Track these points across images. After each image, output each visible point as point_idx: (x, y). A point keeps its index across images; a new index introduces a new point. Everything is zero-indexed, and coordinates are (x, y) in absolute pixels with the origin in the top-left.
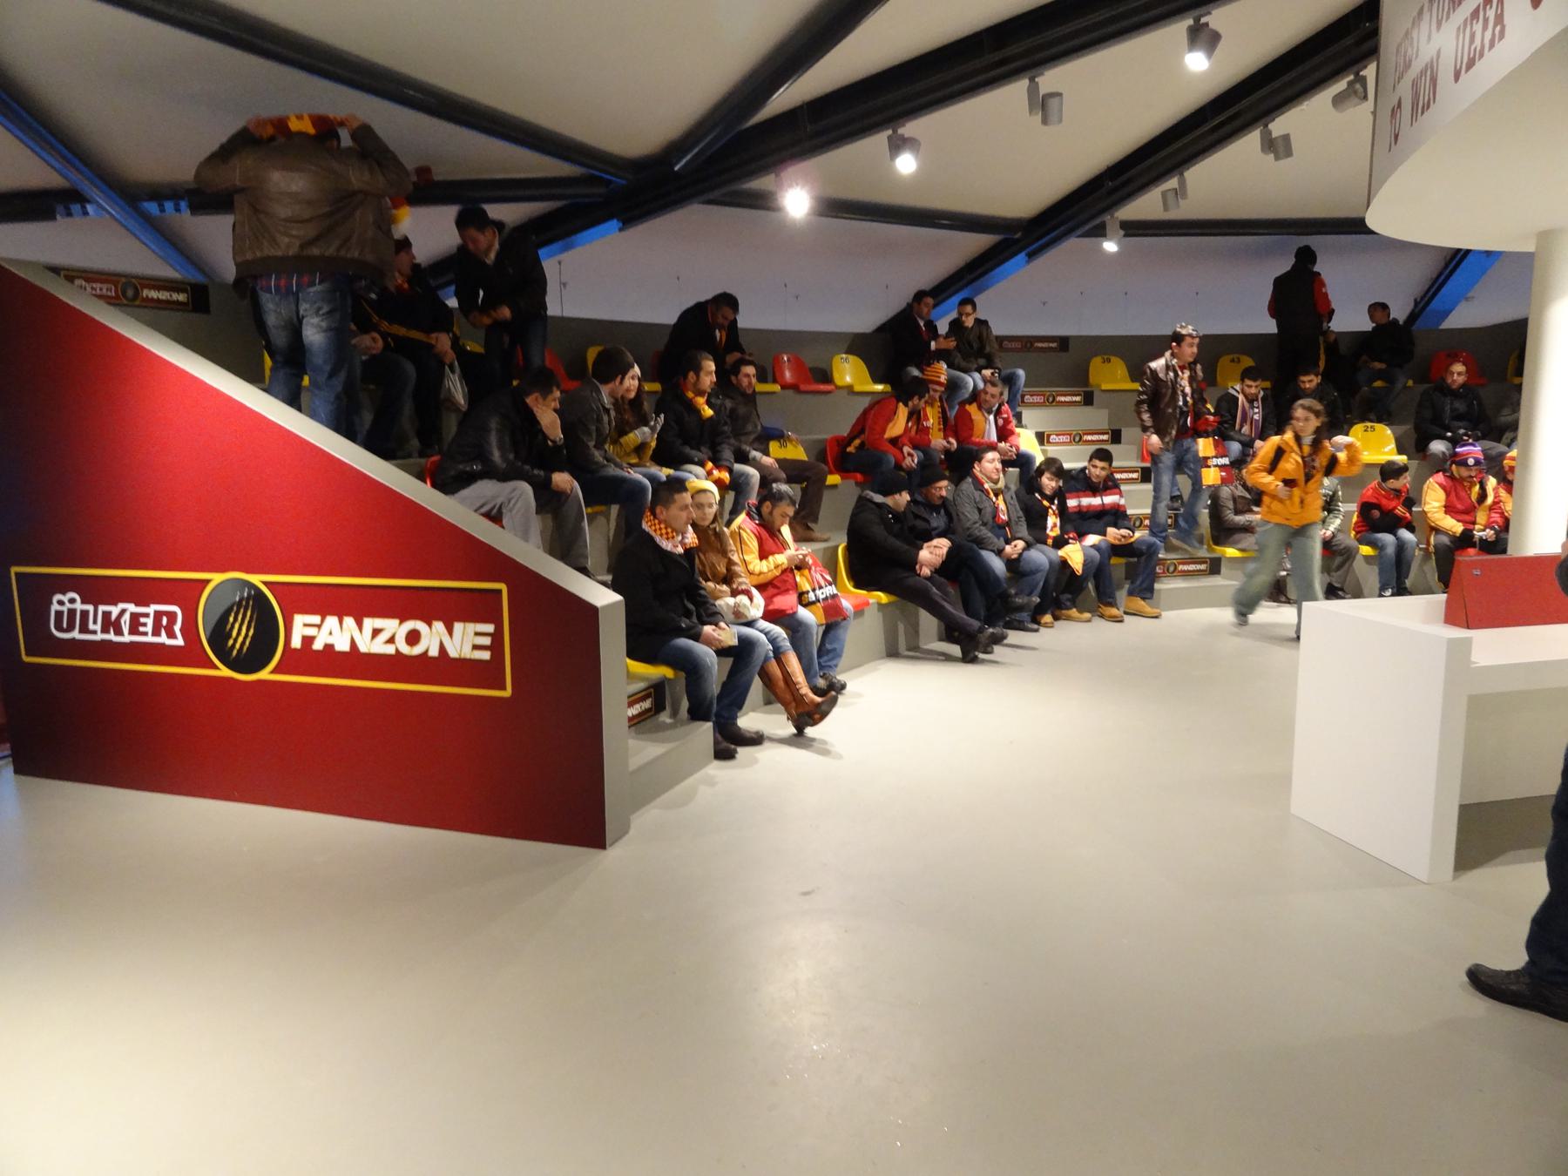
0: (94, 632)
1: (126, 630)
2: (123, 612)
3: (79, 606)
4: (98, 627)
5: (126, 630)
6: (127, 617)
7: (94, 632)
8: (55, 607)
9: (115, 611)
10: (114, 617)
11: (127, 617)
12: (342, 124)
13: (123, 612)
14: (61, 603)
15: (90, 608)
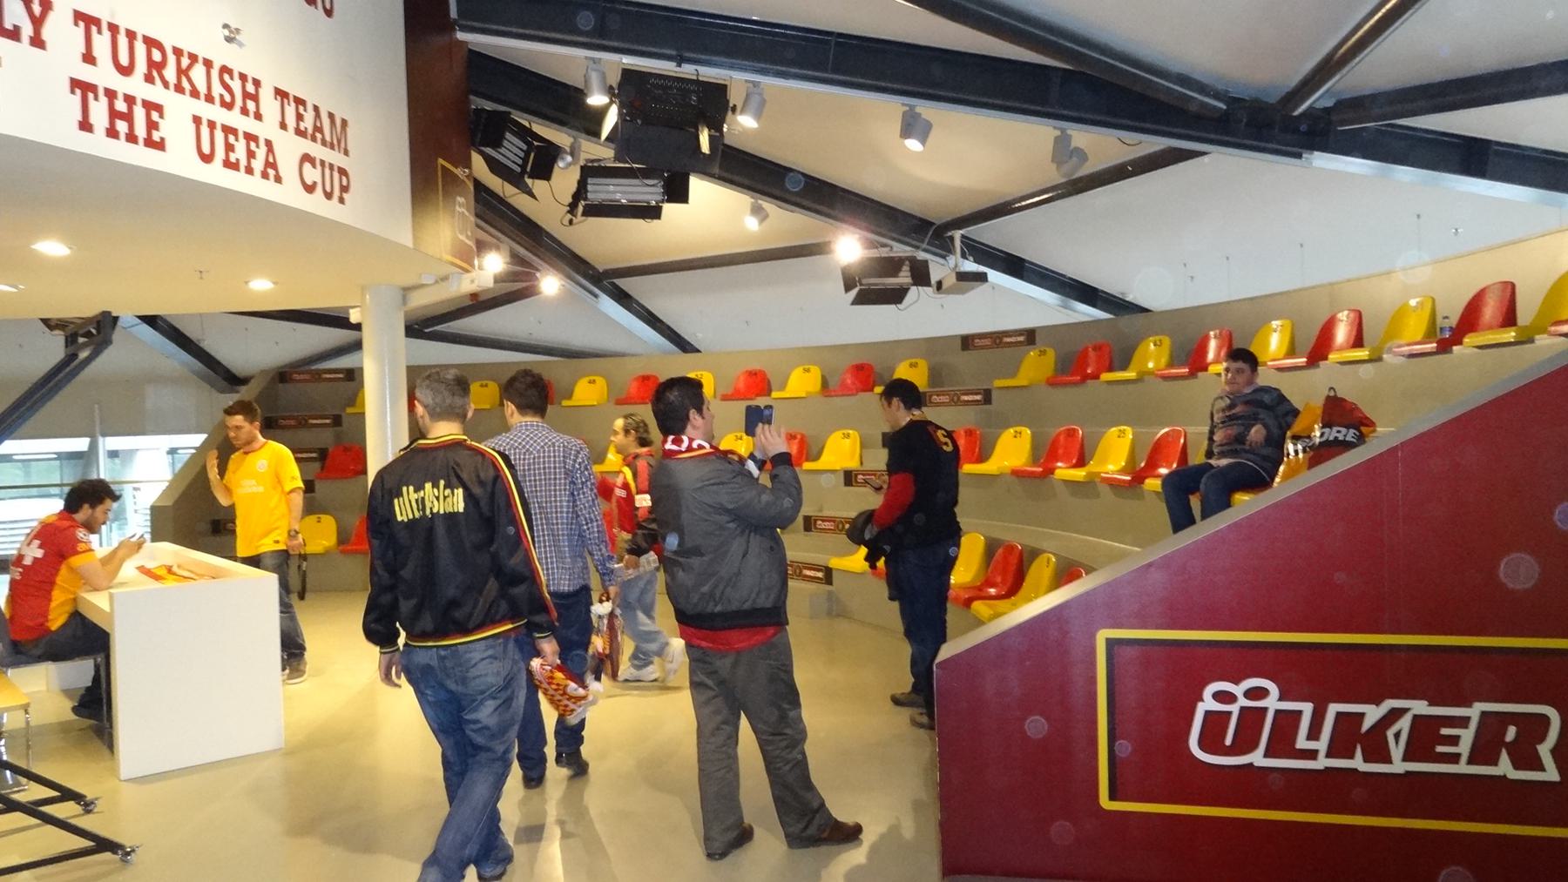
0: (1312, 755)
1: (1397, 752)
2: (1395, 715)
3: (1272, 703)
4: (1322, 745)
5: (1397, 752)
6: (1404, 724)
7: (1312, 755)
8: (1208, 704)
9: (1372, 714)
10: (1367, 724)
11: (1404, 724)
12: (417, 432)
13: (1395, 715)
14: (1221, 697)
15: (1307, 708)
